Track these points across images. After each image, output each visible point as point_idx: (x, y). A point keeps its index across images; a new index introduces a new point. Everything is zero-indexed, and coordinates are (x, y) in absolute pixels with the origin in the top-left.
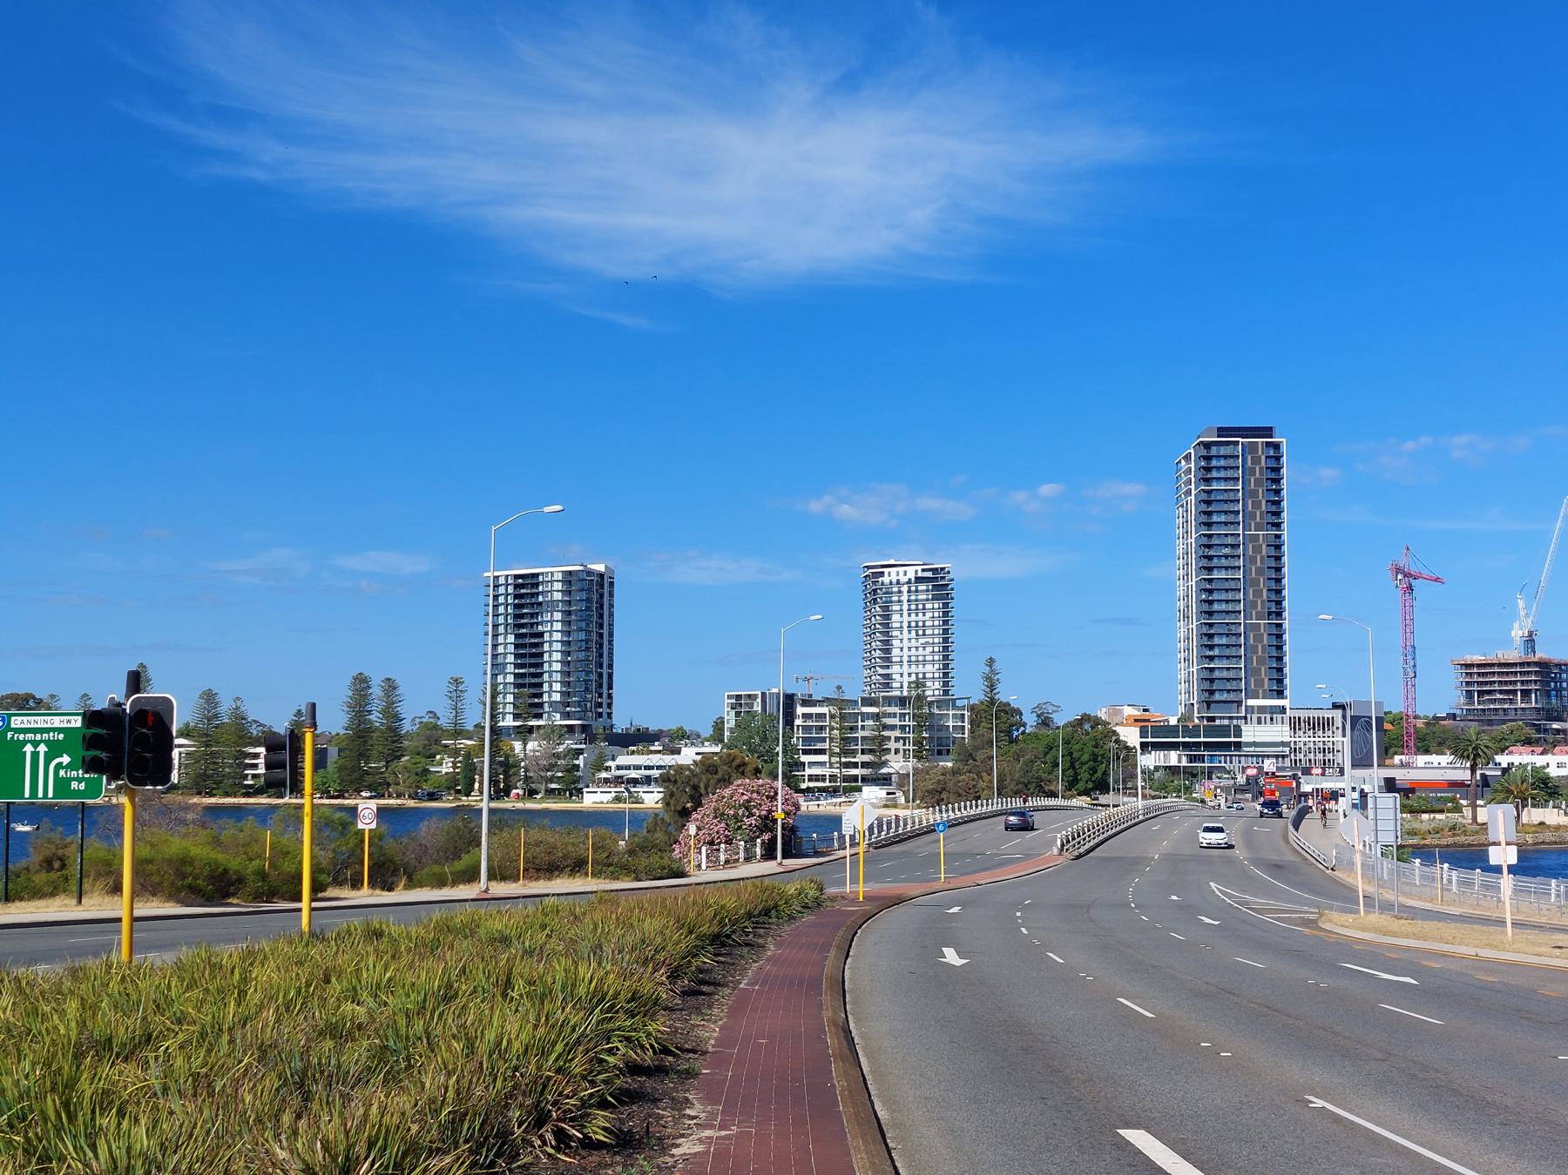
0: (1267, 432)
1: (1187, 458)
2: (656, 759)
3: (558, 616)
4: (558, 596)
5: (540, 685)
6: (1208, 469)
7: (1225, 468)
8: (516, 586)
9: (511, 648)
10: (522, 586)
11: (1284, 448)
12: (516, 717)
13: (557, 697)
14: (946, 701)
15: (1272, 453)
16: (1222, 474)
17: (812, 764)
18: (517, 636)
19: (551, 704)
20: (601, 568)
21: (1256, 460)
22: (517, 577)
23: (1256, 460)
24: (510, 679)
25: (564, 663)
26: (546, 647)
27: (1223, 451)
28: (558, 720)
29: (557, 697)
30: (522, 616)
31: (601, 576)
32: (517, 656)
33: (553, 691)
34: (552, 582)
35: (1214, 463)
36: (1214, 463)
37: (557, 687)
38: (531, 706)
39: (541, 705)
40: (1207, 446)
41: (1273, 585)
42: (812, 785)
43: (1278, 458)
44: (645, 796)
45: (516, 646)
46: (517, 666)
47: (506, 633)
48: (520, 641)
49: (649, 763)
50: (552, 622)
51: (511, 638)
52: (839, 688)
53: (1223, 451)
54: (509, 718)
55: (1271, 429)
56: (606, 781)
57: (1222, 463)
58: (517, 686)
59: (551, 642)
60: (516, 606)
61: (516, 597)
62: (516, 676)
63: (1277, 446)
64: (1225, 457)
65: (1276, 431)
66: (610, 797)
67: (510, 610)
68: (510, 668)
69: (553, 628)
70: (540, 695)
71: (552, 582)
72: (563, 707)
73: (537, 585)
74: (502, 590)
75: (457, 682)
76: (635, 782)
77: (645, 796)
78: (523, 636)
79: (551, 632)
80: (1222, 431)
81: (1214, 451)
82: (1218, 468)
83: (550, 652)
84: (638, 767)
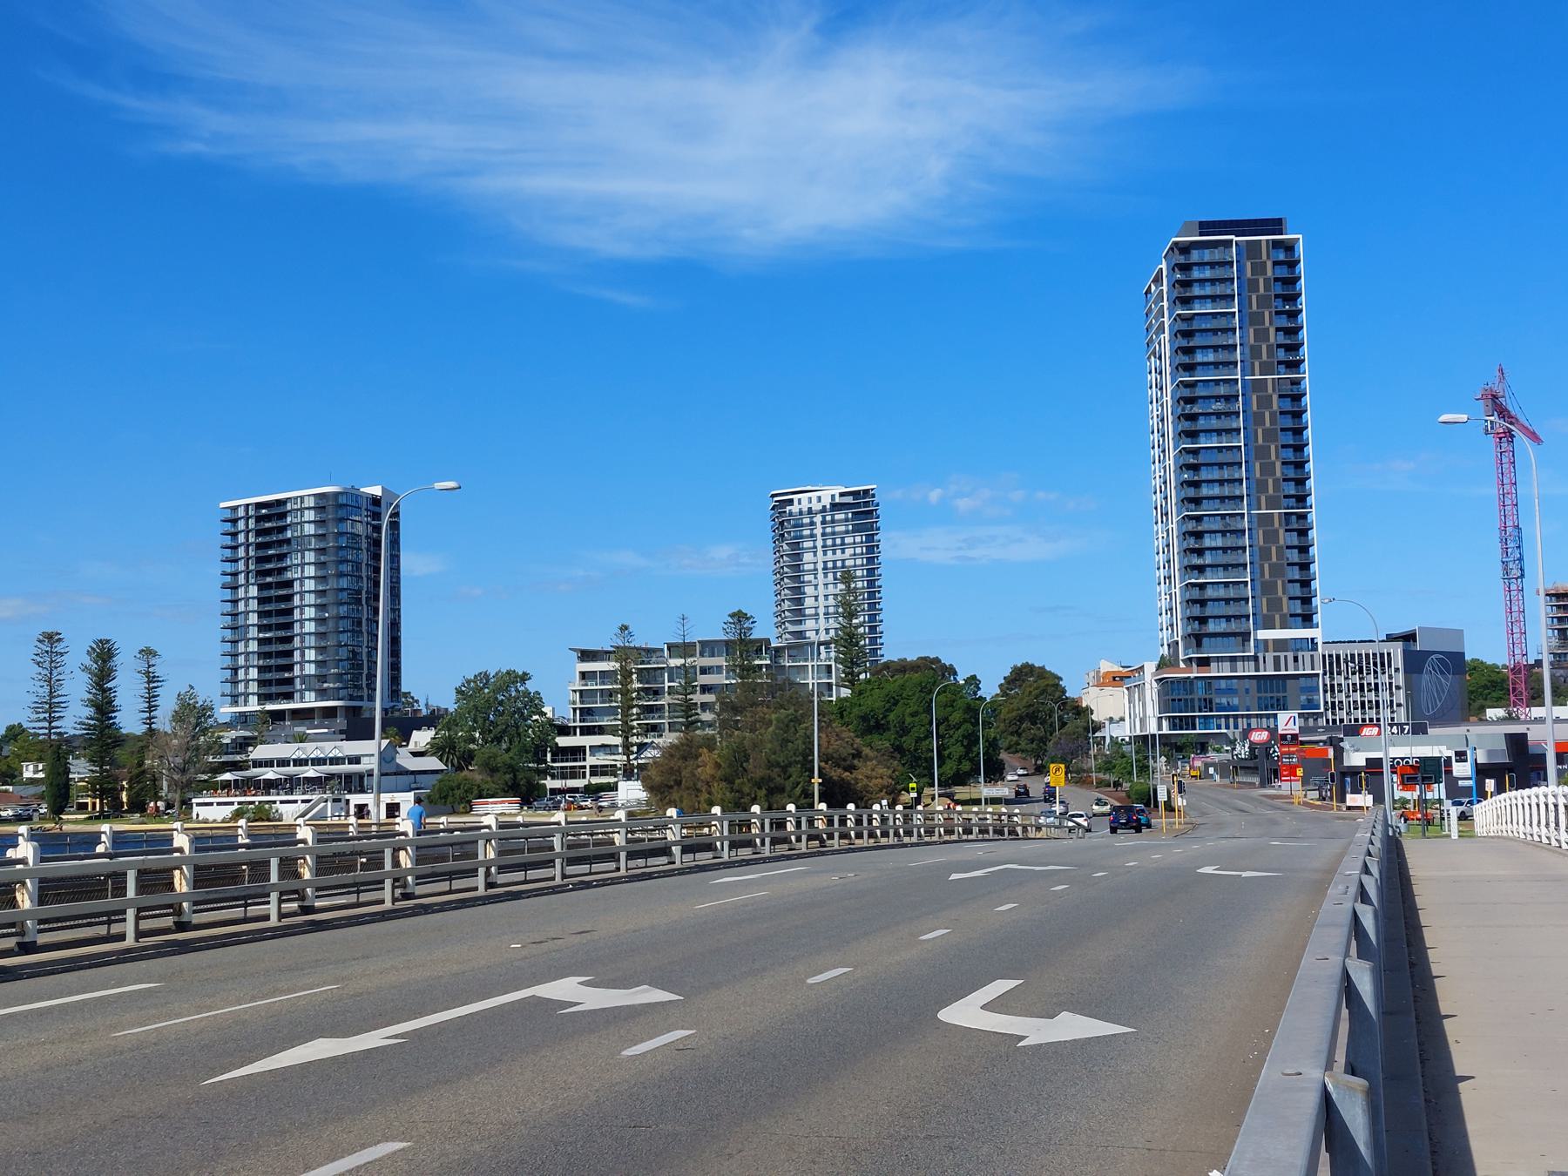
0: (1275, 225)
1: (1158, 280)
2: (311, 750)
3: (310, 557)
4: (310, 529)
5: (290, 654)
6: (1186, 284)
7: (1213, 281)
8: (259, 519)
9: (254, 605)
10: (267, 518)
11: (1301, 249)
12: (264, 698)
13: (310, 669)
14: (800, 646)
15: (1282, 256)
16: (1208, 290)
17: (595, 749)
18: (261, 587)
19: (303, 678)
20: (376, 491)
21: (1259, 268)
22: (259, 506)
23: (1259, 268)
24: (253, 646)
25: (319, 621)
26: (297, 600)
27: (1208, 256)
28: (310, 701)
29: (310, 669)
30: (268, 559)
31: (376, 501)
32: (261, 614)
33: (307, 662)
34: (302, 510)
35: (1196, 274)
36: (1196, 274)
37: (311, 655)
38: (277, 682)
39: (290, 681)
40: (1185, 249)
41: (1283, 322)
42: (595, 780)
43: (1293, 264)
44: (283, 808)
45: (261, 601)
46: (261, 628)
47: (247, 584)
48: (265, 594)
49: (336, 753)
50: (303, 565)
51: (253, 591)
52: (624, 628)
53: (1208, 256)
54: (253, 699)
55: (1279, 222)
56: (226, 785)
57: (1208, 274)
58: (262, 655)
59: (302, 593)
60: (259, 546)
61: (259, 533)
62: (261, 642)
63: (1289, 247)
64: (1212, 265)
65: (1288, 224)
66: (227, 811)
67: (252, 553)
68: (253, 633)
69: (305, 573)
70: (290, 668)
71: (302, 510)
72: (318, 684)
73: (283, 516)
74: (241, 525)
75: (51, 638)
76: (270, 786)
77: (283, 808)
78: (268, 586)
79: (302, 579)
80: (1206, 227)
81: (1195, 256)
82: (1202, 281)
83: (302, 607)
84: (318, 762)
